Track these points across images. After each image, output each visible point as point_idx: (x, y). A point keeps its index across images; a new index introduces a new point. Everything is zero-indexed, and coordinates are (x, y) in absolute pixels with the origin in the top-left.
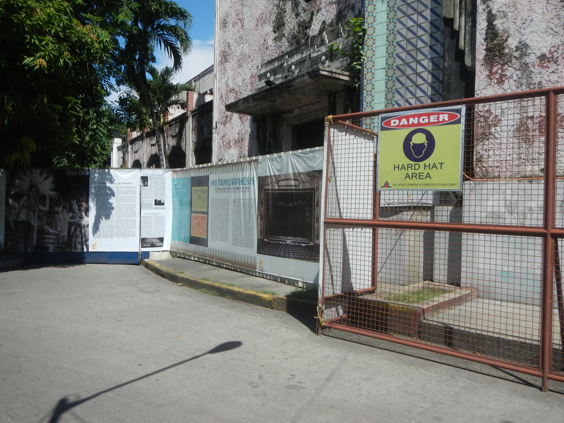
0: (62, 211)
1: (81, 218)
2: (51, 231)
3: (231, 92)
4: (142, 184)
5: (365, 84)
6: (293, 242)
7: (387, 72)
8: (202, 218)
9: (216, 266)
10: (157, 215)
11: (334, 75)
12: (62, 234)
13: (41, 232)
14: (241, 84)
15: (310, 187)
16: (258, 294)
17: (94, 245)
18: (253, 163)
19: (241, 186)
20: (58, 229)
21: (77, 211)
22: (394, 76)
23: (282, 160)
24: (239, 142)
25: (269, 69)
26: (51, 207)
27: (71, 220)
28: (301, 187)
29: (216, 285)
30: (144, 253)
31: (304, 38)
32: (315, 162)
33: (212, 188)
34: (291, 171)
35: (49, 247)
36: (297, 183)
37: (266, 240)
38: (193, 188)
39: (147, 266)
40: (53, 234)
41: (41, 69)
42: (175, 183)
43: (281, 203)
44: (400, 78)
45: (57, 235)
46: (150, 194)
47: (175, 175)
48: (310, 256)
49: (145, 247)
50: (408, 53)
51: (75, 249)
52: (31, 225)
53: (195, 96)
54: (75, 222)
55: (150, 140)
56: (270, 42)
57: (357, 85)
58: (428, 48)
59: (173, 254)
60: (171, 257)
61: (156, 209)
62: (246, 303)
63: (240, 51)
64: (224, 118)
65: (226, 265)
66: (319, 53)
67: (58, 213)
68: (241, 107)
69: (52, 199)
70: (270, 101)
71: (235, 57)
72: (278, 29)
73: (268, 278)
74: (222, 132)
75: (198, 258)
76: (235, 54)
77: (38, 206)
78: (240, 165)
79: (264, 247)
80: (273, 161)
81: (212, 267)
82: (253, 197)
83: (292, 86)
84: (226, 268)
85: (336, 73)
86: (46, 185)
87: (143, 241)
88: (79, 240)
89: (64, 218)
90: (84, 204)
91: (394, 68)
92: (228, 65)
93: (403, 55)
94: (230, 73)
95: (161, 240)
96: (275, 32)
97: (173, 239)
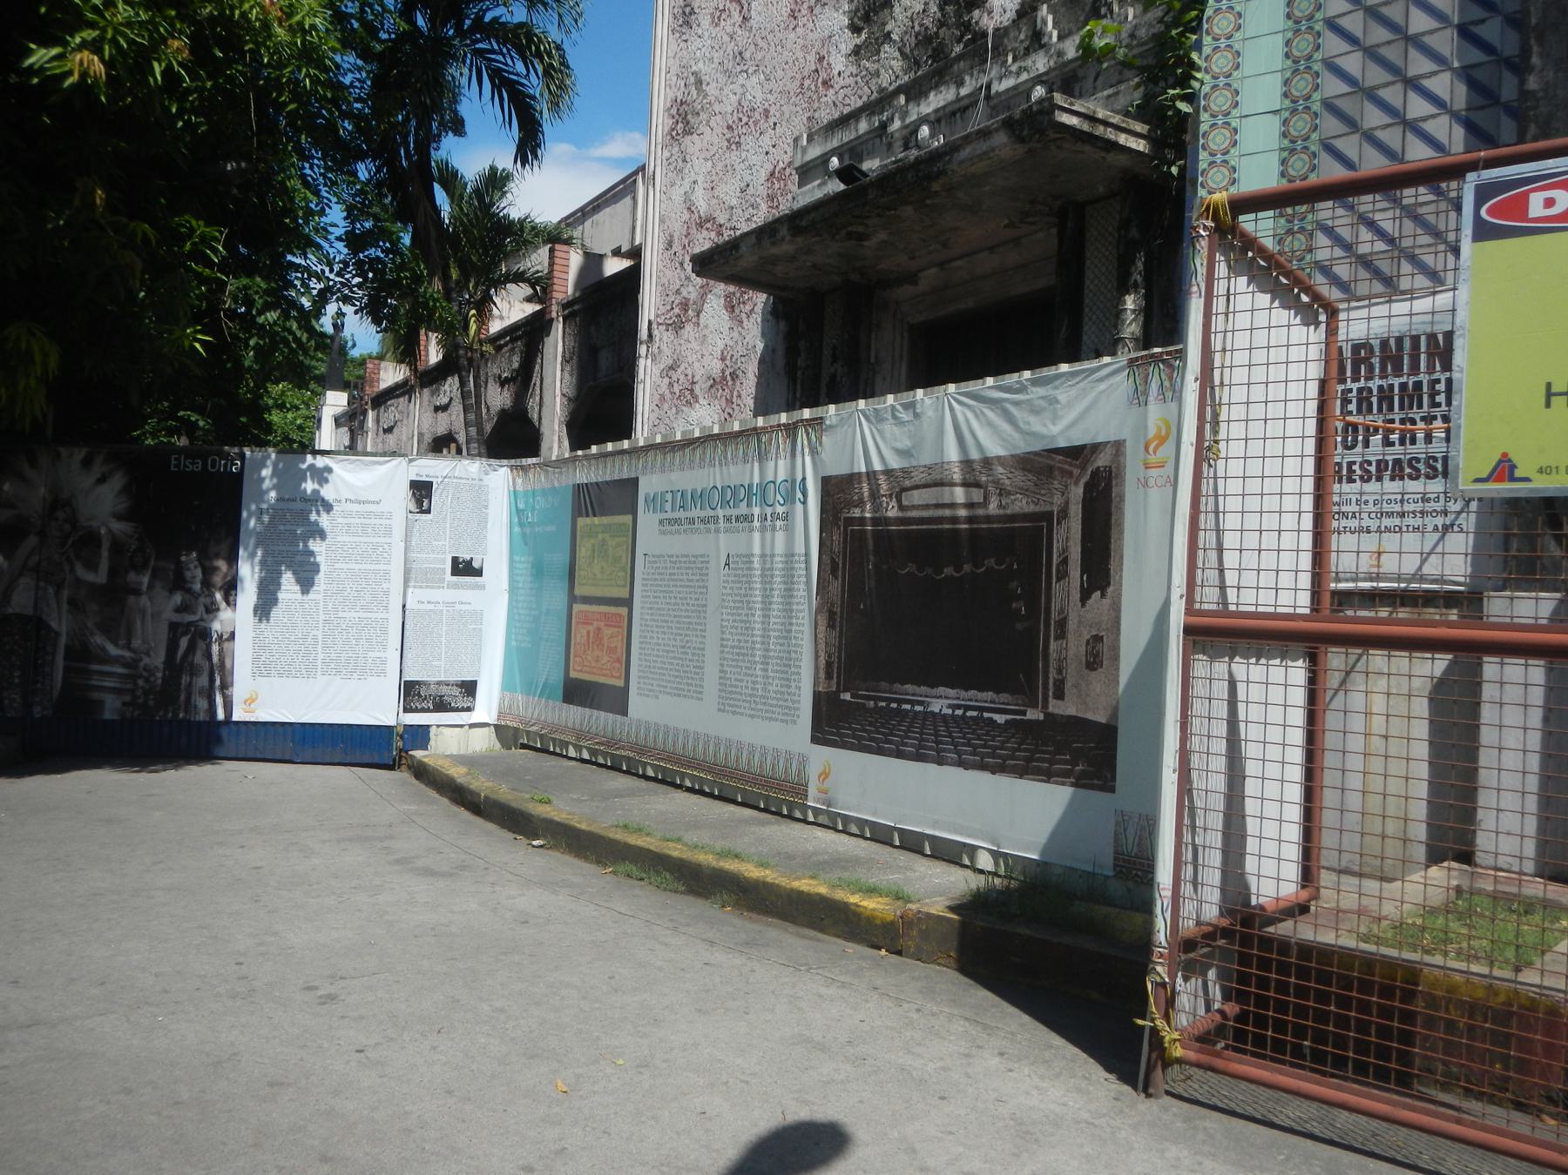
0: (151, 586)
1: (212, 609)
2: (113, 650)
3: (700, 225)
4: (412, 506)
5: (1202, 165)
6: (959, 706)
7: (1285, 122)
8: (609, 620)
9: (655, 780)
10: (458, 607)
11: (1100, 130)
12: (146, 660)
13: (81, 654)
14: (734, 202)
15: (1032, 508)
16: (840, 895)
17: (249, 701)
18: (801, 432)
19: (756, 511)
20: (136, 643)
21: (197, 587)
22: (1315, 136)
23: (916, 416)
24: (723, 382)
25: (835, 143)
26: (113, 572)
27: (177, 618)
28: (993, 508)
29: (675, 854)
30: (409, 728)
31: (959, 41)
32: (1054, 420)
33: (647, 520)
34: (953, 454)
35: (102, 702)
36: (977, 495)
37: (847, 696)
38: (581, 521)
39: (422, 773)
40: (117, 660)
41: (85, 87)
42: (521, 506)
43: (911, 568)
44: (1339, 144)
45: (132, 665)
46: (441, 538)
47: (519, 481)
48: (1029, 760)
49: (416, 710)
50: (1372, 53)
51: (186, 711)
52: (49, 626)
53: (575, 260)
54: (190, 624)
55: (433, 394)
56: (839, 62)
57: (1174, 170)
58: (1451, 34)
59: (503, 732)
60: (498, 746)
61: (456, 586)
62: (792, 928)
63: (734, 99)
64: (677, 311)
65: (693, 778)
66: (1024, 76)
67: (137, 592)
68: (748, 259)
69: (117, 547)
70: (850, 236)
71: (718, 118)
72: (867, 18)
73: (854, 829)
74: (667, 351)
75: (593, 752)
76: (717, 108)
77: (72, 569)
78: (754, 442)
79: (832, 722)
80: (880, 420)
81: (643, 784)
82: (800, 548)
83: (942, 173)
84: (691, 790)
85: (1106, 123)
86: (102, 501)
87: (411, 693)
88: (203, 681)
89: (156, 609)
90: (222, 565)
91: (1316, 107)
92: (693, 144)
93: (1353, 63)
94: (699, 168)
95: (469, 688)
96: (855, 29)
97: (507, 685)
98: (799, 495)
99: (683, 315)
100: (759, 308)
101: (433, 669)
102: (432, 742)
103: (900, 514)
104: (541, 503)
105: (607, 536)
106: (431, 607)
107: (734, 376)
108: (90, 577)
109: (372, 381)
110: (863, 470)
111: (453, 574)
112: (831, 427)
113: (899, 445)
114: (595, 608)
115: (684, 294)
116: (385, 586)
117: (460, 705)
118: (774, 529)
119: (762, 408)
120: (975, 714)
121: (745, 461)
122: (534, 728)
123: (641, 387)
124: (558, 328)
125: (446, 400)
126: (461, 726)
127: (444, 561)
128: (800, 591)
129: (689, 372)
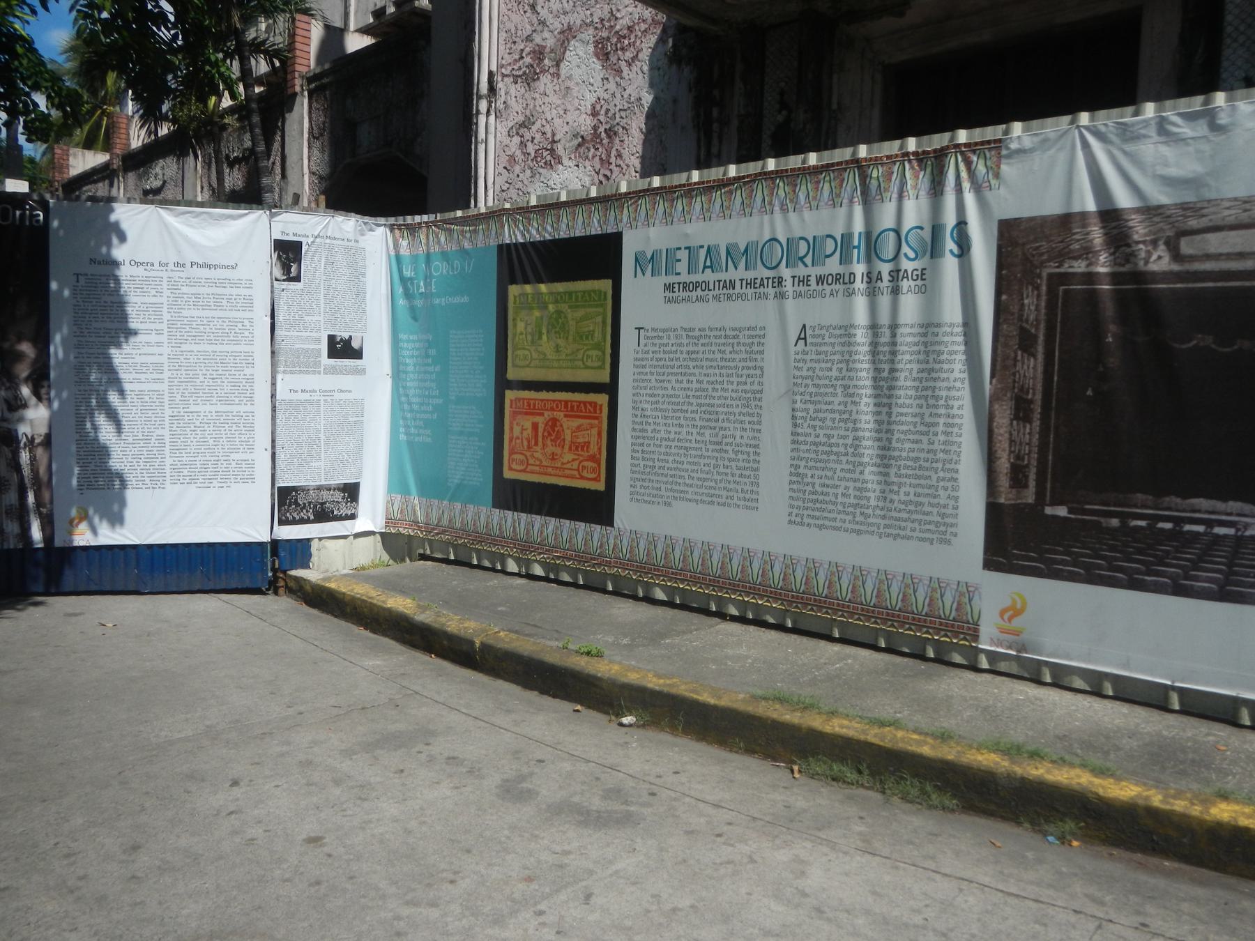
4: (278, 272)
8: (572, 410)
10: (337, 396)
23: (1215, 127)
24: (598, 140)
37: (1062, 511)
38: (514, 290)
39: (323, 600)
42: (408, 273)
46: (311, 313)
49: (294, 522)
53: (316, 32)
55: (140, 178)
60: (386, 557)
61: (333, 371)
64: (528, 60)
65: (743, 605)
74: (516, 106)
78: (852, 179)
79: (1015, 541)
80: (1136, 138)
82: (952, 311)
87: (287, 501)
90: (26, 348)
95: (351, 492)
98: (950, 245)
99: (537, 64)
100: (645, 55)
102: (314, 559)
103: (1176, 267)
104: (440, 268)
105: (564, 307)
106: (306, 396)
107: (611, 133)
109: (61, 167)
110: (1091, 206)
111: (330, 356)
112: (1020, 151)
113: (1173, 171)
114: (544, 395)
115: (538, 39)
116: (248, 371)
117: (343, 512)
118: (896, 291)
119: (646, 173)
120: (1168, 526)
121: (835, 201)
122: (445, 537)
123: (481, 148)
125: (157, 183)
126: (345, 537)
127: (319, 340)
128: (957, 369)
129: (548, 129)
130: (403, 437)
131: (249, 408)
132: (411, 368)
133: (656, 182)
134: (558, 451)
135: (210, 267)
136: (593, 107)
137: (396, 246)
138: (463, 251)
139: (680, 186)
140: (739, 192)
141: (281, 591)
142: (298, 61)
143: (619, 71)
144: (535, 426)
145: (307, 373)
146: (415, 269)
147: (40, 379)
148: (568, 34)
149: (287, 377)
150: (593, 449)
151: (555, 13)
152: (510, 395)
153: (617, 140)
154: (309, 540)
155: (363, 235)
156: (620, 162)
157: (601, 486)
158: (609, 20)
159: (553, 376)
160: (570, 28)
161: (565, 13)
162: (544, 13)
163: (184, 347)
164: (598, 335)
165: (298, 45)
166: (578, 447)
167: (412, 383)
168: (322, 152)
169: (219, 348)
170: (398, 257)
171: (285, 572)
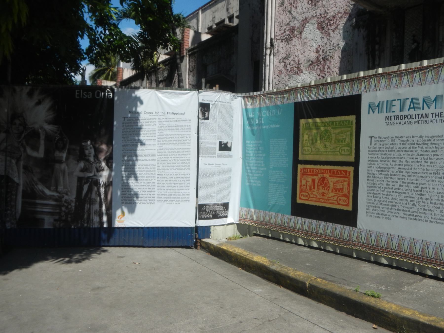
0: (67, 158)
1: (100, 170)
2: (48, 192)
4: (200, 116)
8: (333, 174)
10: (222, 166)
12: (66, 197)
13: (31, 195)
20: (60, 188)
21: (92, 159)
24: (320, 62)
26: (47, 152)
27: (82, 175)
35: (43, 220)
38: (302, 122)
39: (218, 253)
40: (51, 198)
42: (251, 116)
45: (59, 199)
47: (249, 104)
49: (204, 219)
51: (88, 223)
52: (13, 182)
53: (191, 33)
54: (89, 177)
60: (238, 234)
61: (220, 156)
64: (288, 33)
67: (60, 162)
69: (49, 138)
77: (25, 151)
86: (40, 115)
88: (96, 207)
89: (70, 171)
90: (104, 147)
95: (226, 206)
99: (291, 34)
100: (341, 26)
101: (210, 198)
105: (329, 128)
106: (210, 167)
107: (325, 59)
108: (35, 154)
114: (318, 167)
115: (292, 24)
116: (188, 156)
117: (223, 215)
123: (267, 68)
124: (187, 60)
126: (223, 225)
127: (216, 143)
129: (296, 59)
130: (247, 184)
131: (188, 171)
132: (251, 155)
133: (345, 77)
134: (326, 191)
135: (174, 114)
136: (317, 49)
137: (246, 104)
138: (277, 107)
139: (395, 72)
140: (430, 73)
141: (199, 247)
142: (185, 44)
143: (329, 34)
144: (313, 181)
145: (211, 157)
146: (254, 114)
147: (109, 160)
148: (305, 21)
149: (203, 159)
150: (345, 191)
151: (299, 13)
152: (300, 167)
153: (328, 62)
154: (210, 226)
155: (232, 100)
156: (329, 70)
157: (350, 208)
158: (324, 14)
159: (323, 158)
160: (306, 19)
161: (304, 13)
162: (294, 14)
163: (164, 146)
164: (348, 140)
165: (185, 39)
166: (336, 190)
167: (252, 160)
168: (193, 76)
169: (177, 147)
170: (246, 110)
171: (200, 240)
